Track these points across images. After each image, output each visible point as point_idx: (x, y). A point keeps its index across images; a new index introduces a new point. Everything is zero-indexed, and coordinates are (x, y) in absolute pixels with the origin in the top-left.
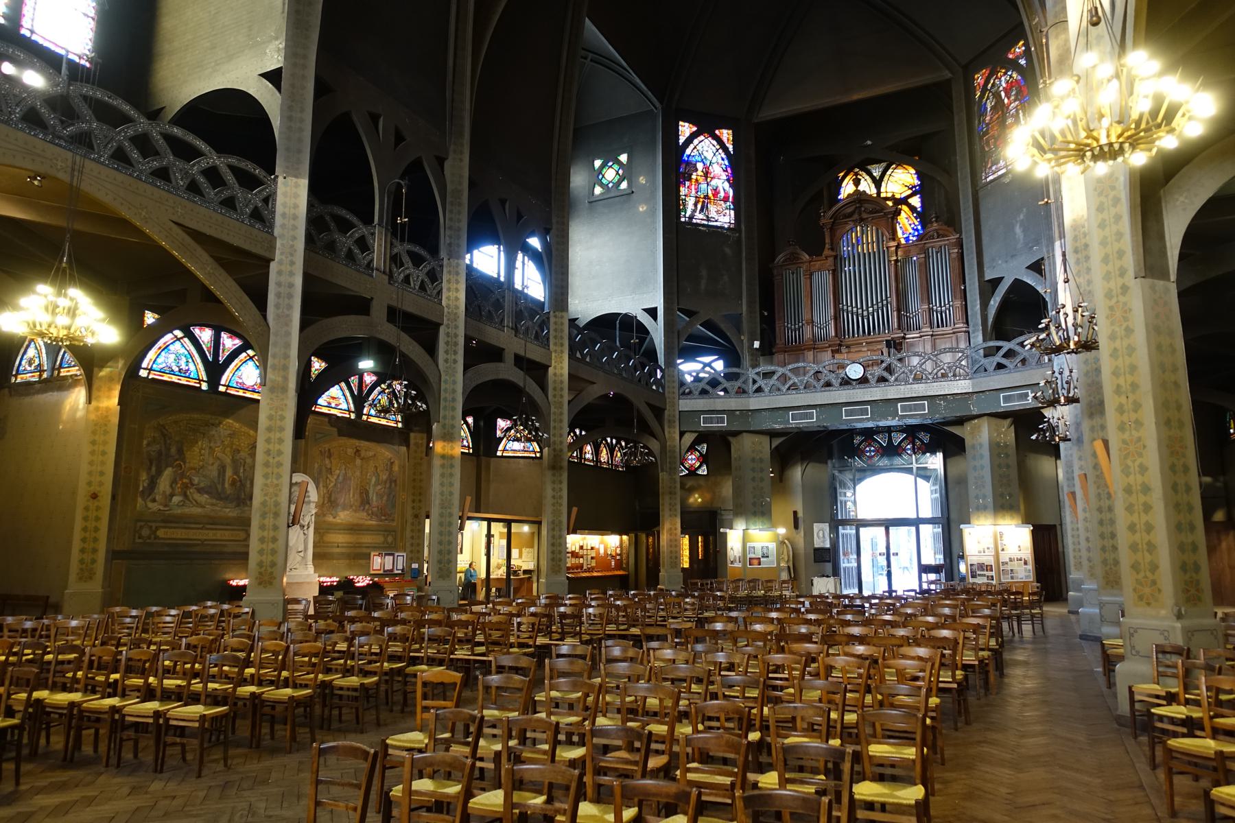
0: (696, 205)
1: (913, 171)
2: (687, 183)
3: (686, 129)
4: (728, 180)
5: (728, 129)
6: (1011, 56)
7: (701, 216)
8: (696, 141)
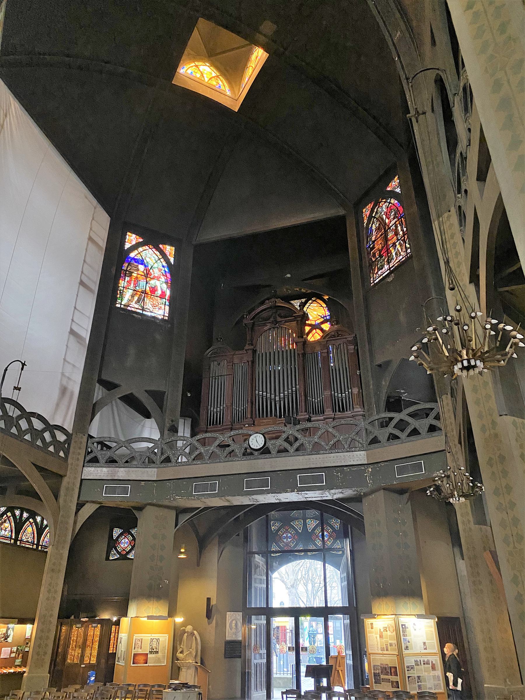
0: (133, 296)
1: (325, 305)
2: (127, 279)
3: (131, 239)
4: (166, 283)
5: (171, 245)
6: (389, 189)
7: (137, 306)
8: (140, 249)
